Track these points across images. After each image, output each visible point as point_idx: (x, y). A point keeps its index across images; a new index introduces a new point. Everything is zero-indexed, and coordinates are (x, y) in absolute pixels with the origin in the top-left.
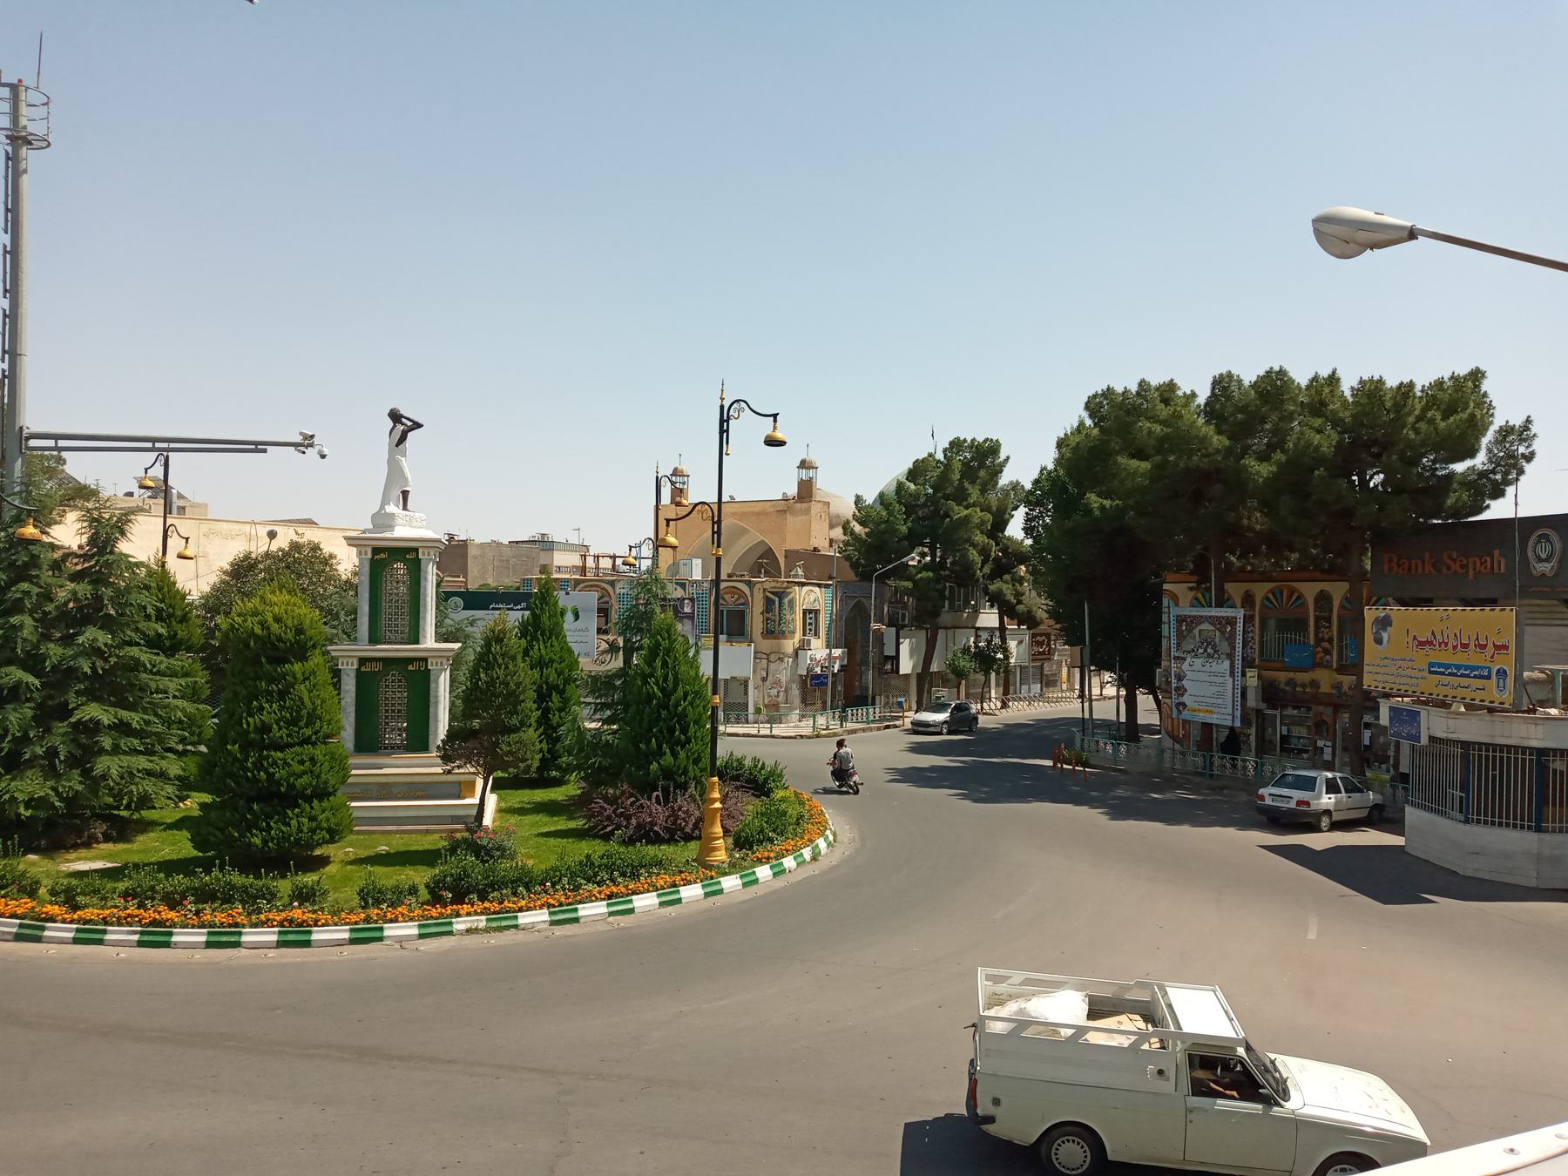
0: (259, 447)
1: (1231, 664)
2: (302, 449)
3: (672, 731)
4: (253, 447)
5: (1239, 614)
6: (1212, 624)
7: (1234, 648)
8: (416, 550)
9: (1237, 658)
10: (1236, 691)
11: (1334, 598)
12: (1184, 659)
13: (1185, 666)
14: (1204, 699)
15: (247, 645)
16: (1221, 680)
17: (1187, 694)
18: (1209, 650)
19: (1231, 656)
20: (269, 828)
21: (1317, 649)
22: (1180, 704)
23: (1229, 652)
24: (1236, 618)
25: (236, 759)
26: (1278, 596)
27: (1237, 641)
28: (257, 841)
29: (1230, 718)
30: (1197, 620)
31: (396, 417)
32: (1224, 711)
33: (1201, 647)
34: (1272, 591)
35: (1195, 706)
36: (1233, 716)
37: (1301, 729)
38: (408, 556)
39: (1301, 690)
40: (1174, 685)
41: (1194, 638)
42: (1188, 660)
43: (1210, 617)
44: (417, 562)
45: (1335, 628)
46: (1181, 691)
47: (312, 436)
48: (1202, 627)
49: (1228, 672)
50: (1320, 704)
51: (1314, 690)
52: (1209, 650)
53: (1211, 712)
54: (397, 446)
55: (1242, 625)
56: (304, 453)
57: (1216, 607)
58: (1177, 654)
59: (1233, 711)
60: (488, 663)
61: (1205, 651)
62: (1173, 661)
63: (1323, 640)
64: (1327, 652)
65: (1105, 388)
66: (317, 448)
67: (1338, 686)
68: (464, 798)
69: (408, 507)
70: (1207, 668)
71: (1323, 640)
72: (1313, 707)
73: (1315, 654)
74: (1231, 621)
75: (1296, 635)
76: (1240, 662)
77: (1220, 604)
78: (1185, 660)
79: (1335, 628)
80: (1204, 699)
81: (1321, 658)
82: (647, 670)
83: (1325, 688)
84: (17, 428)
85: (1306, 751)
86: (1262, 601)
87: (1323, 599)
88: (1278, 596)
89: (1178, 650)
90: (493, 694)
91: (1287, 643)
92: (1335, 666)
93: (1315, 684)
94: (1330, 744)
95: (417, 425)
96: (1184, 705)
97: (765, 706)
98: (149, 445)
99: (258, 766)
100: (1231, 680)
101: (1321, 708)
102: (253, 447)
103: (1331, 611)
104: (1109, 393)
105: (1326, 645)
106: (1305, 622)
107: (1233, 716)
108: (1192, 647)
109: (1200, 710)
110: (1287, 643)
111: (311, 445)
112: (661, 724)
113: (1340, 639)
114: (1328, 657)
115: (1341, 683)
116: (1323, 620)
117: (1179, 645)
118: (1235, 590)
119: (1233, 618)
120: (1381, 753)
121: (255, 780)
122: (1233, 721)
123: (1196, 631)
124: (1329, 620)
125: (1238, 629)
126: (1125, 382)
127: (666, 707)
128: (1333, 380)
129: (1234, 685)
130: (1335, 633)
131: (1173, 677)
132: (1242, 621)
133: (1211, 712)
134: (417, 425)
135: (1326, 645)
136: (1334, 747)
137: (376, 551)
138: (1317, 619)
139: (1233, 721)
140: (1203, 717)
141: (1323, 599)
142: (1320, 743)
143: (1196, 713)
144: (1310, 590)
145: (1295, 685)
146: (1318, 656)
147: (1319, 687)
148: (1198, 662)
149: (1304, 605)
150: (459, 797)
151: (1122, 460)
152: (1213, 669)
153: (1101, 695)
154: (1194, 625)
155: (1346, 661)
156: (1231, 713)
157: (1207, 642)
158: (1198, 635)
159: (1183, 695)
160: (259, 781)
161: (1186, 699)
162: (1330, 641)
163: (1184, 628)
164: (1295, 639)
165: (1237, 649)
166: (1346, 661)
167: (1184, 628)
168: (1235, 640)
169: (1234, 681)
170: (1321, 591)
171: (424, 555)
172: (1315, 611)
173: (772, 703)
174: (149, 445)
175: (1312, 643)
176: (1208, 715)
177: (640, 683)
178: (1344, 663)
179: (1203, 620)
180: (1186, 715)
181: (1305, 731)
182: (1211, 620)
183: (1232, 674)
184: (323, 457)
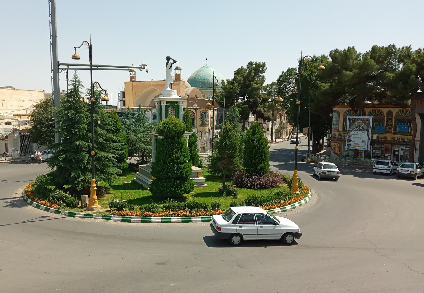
0: (129, 68)
1: (367, 132)
2: (141, 69)
3: (261, 156)
4: (127, 68)
5: (371, 118)
6: (361, 121)
7: (368, 128)
8: (178, 102)
9: (370, 131)
10: (369, 140)
11: (367, 112)
12: (351, 131)
13: (351, 133)
14: (357, 143)
15: (170, 133)
16: (364, 137)
17: (351, 141)
18: (360, 128)
19: (368, 130)
20: (181, 188)
21: (387, 128)
22: (349, 144)
23: (367, 129)
24: (370, 119)
25: (171, 168)
26: (374, 112)
27: (370, 126)
28: (179, 191)
29: (367, 148)
30: (357, 120)
31: (168, 59)
32: (364, 146)
33: (357, 127)
34: (372, 111)
35: (355, 145)
36: (368, 148)
37: (379, 151)
38: (175, 104)
39: (381, 139)
40: (347, 139)
41: (355, 125)
42: (353, 131)
43: (361, 119)
44: (178, 106)
45: (393, 121)
46: (349, 140)
47: (147, 65)
48: (358, 122)
49: (367, 135)
50: (387, 144)
51: (385, 140)
52: (360, 128)
53: (360, 146)
54: (170, 68)
55: (372, 121)
56: (141, 70)
57: (362, 116)
58: (349, 130)
59: (368, 146)
60: (228, 137)
61: (359, 128)
62: (347, 132)
63: (389, 125)
64: (391, 129)
65: (336, 49)
66: (146, 69)
67: (394, 138)
68: (199, 177)
69: (172, 89)
70: (359, 134)
71: (389, 125)
72: (385, 144)
73: (386, 129)
74: (368, 120)
75: (380, 123)
76: (371, 132)
77: (360, 115)
78: (352, 131)
79: (393, 121)
80: (357, 143)
81: (389, 130)
82: (253, 138)
83: (389, 139)
84: (57, 62)
85: (380, 157)
86: (368, 113)
87: (390, 113)
88: (374, 112)
89: (349, 128)
90: (231, 147)
91: (376, 125)
92: (393, 132)
93: (385, 138)
94: (390, 155)
95: (175, 62)
96: (350, 145)
97: (201, 148)
98: (99, 68)
99: (178, 170)
100: (367, 137)
101: (387, 145)
102: (127, 68)
103: (392, 116)
104: (337, 51)
105: (390, 126)
106: (384, 119)
107: (368, 148)
108: (354, 128)
109: (356, 146)
110: (376, 125)
111: (144, 68)
112: (259, 154)
113: (395, 124)
114: (390, 130)
115: (395, 137)
116: (389, 119)
117: (349, 127)
118: (368, 110)
119: (369, 119)
120: (406, 157)
121: (177, 174)
122: (368, 149)
123: (356, 123)
124: (391, 119)
125: (370, 122)
126: (342, 48)
127: (259, 149)
128: (387, 47)
129: (368, 139)
130: (393, 123)
131: (347, 136)
132: (372, 120)
133: (360, 146)
134: (175, 62)
135: (390, 126)
136: (391, 156)
137: (167, 102)
138: (387, 119)
139: (368, 149)
140: (357, 148)
141: (390, 113)
142: (386, 155)
143: (354, 147)
144: (385, 111)
145: (379, 138)
146: (387, 130)
147: (387, 139)
148: (356, 132)
149: (383, 114)
150: (197, 177)
151: (344, 71)
152: (361, 134)
153: (276, 141)
154: (355, 121)
155: (397, 131)
156: (367, 147)
157: (359, 126)
158: (356, 124)
159: (350, 142)
160: (178, 174)
161: (351, 143)
162: (392, 125)
163: (352, 122)
164: (381, 125)
165: (370, 128)
166: (397, 131)
167: (352, 122)
168: (369, 125)
169: (368, 137)
170: (389, 110)
171: (181, 104)
172: (387, 117)
173: (203, 147)
174: (99, 68)
175: (385, 126)
176: (359, 147)
177: (251, 142)
178: (409, 132)
179: (358, 119)
180: (351, 147)
181: (380, 151)
182: (362, 120)
183: (368, 135)
184: (147, 72)
